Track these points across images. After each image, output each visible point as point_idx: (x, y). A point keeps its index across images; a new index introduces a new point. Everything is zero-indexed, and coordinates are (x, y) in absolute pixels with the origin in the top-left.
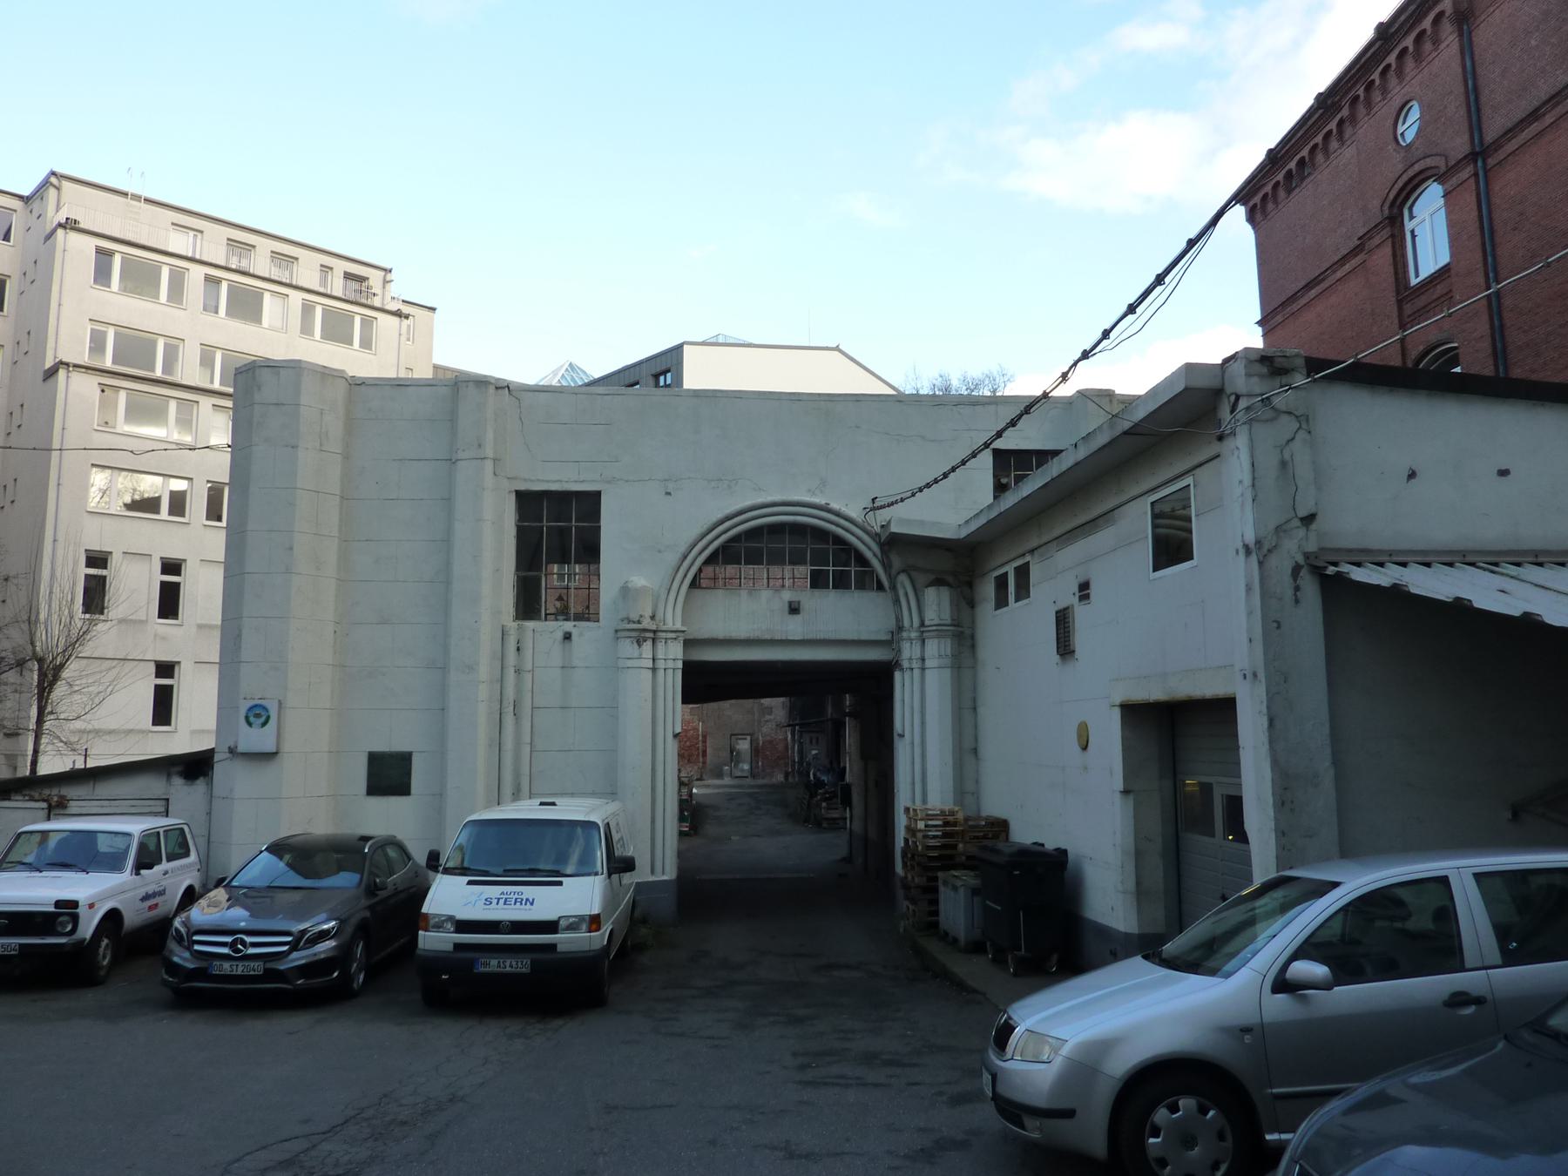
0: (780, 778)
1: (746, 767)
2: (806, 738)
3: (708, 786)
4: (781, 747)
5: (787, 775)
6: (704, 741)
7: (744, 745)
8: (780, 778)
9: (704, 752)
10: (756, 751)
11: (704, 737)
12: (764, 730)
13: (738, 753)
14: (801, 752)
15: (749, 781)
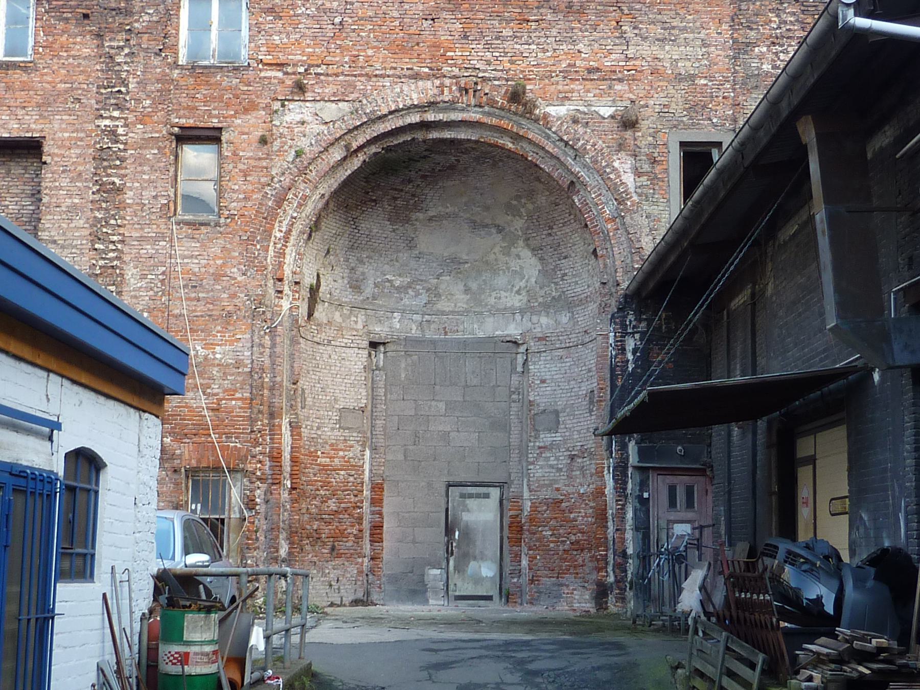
0: (578, 601)
1: (488, 570)
2: (659, 486)
3: (375, 621)
4: (583, 516)
5: (601, 593)
6: (376, 501)
7: (482, 514)
8: (578, 601)
9: (377, 529)
10: (514, 530)
11: (377, 488)
12: (538, 472)
13: (467, 534)
14: (643, 527)
15: (496, 609)
